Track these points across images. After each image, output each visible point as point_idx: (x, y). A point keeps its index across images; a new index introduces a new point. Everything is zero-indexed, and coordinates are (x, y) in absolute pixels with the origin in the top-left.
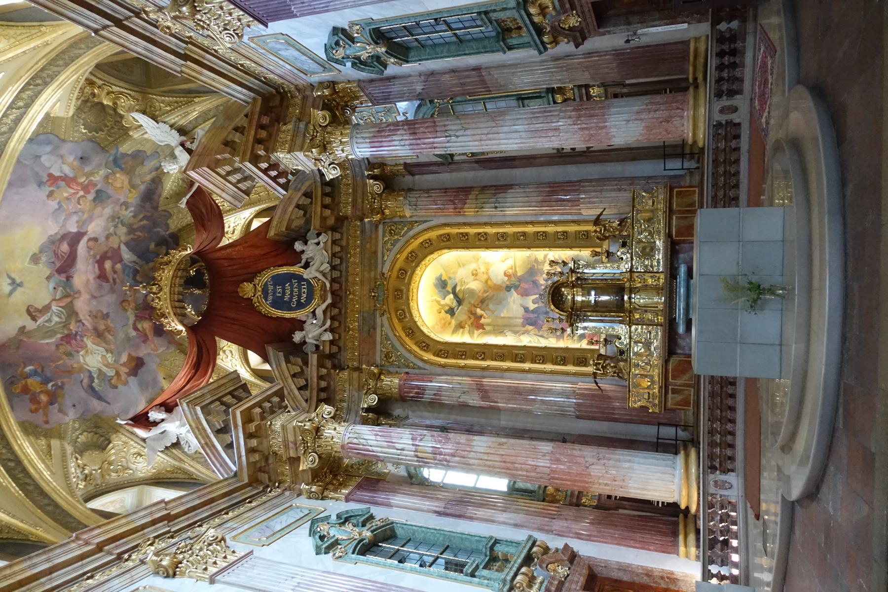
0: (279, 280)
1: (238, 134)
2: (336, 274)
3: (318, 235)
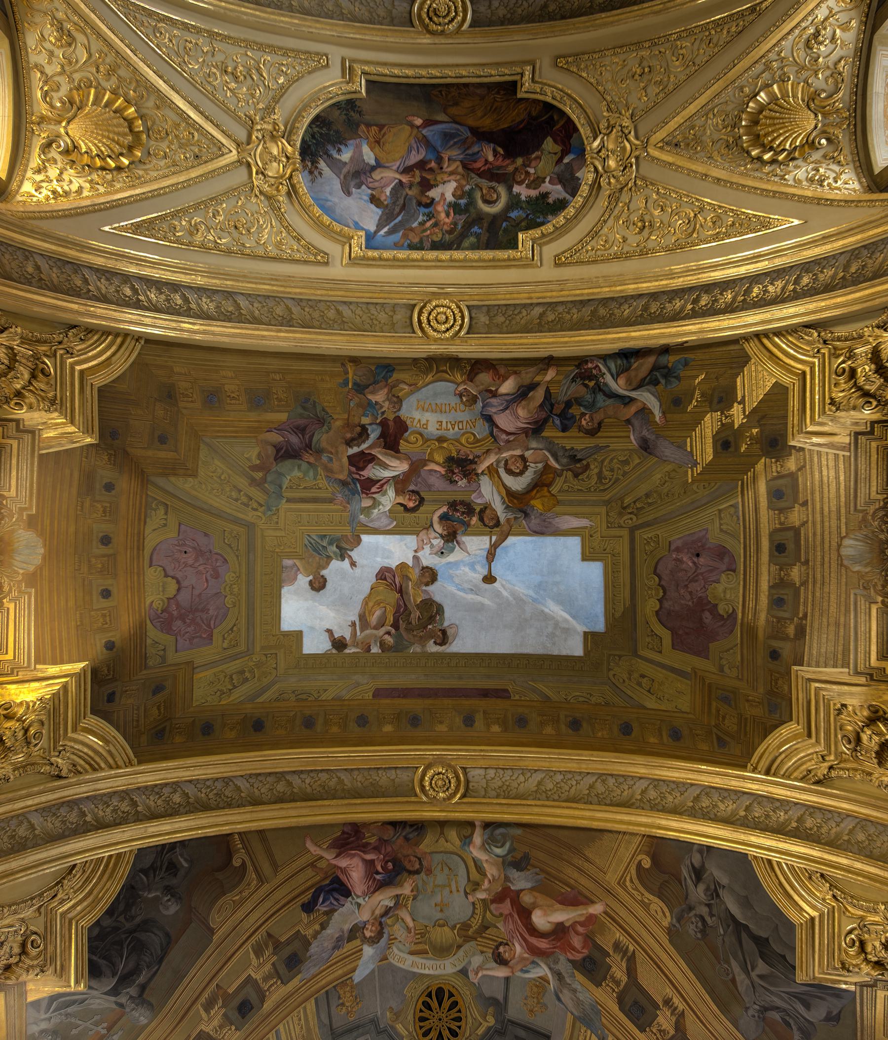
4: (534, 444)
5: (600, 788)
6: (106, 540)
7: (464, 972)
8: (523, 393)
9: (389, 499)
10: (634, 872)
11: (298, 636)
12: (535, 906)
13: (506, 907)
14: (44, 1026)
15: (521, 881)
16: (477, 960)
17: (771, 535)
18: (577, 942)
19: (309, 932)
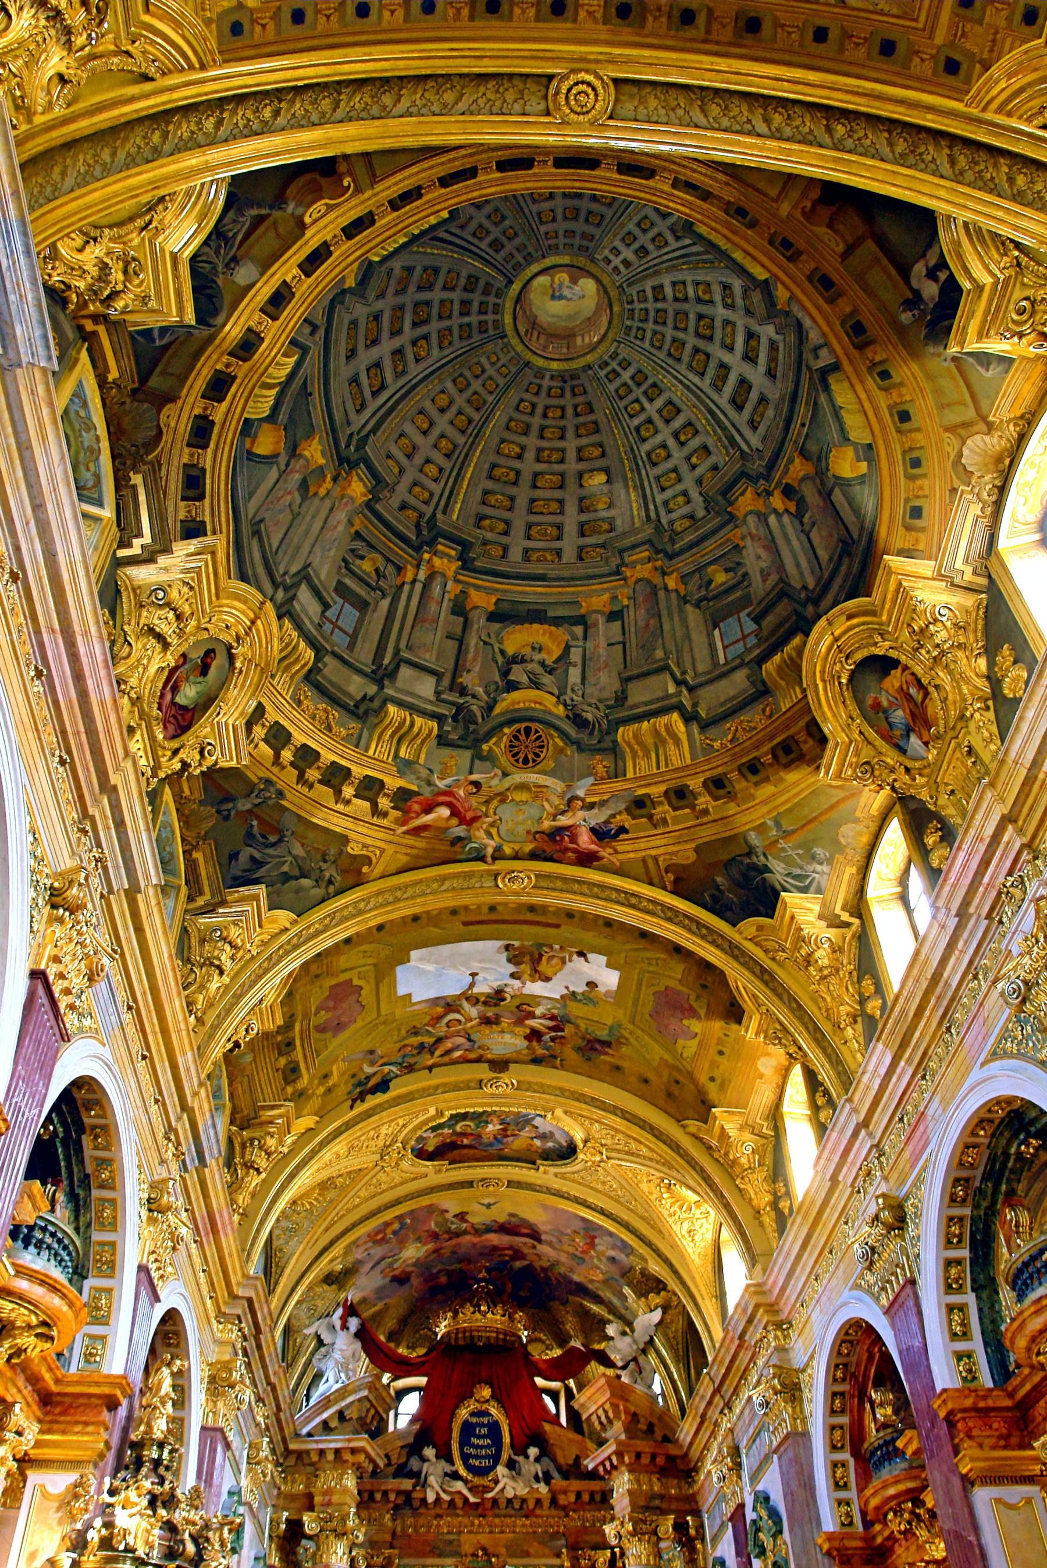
0: (494, 1428)
1: (645, 1428)
2: (502, 1503)
3: (547, 1478)
4: (442, 1034)
5: (399, 894)
6: (721, 1053)
7: (505, 774)
8: (448, 1052)
9: (538, 1011)
10: (374, 860)
11: (609, 965)
12: (448, 819)
13: (469, 815)
14: (819, 868)
15: (460, 831)
16: (495, 782)
17: (295, 1048)
18: (416, 807)
19: (625, 816)
